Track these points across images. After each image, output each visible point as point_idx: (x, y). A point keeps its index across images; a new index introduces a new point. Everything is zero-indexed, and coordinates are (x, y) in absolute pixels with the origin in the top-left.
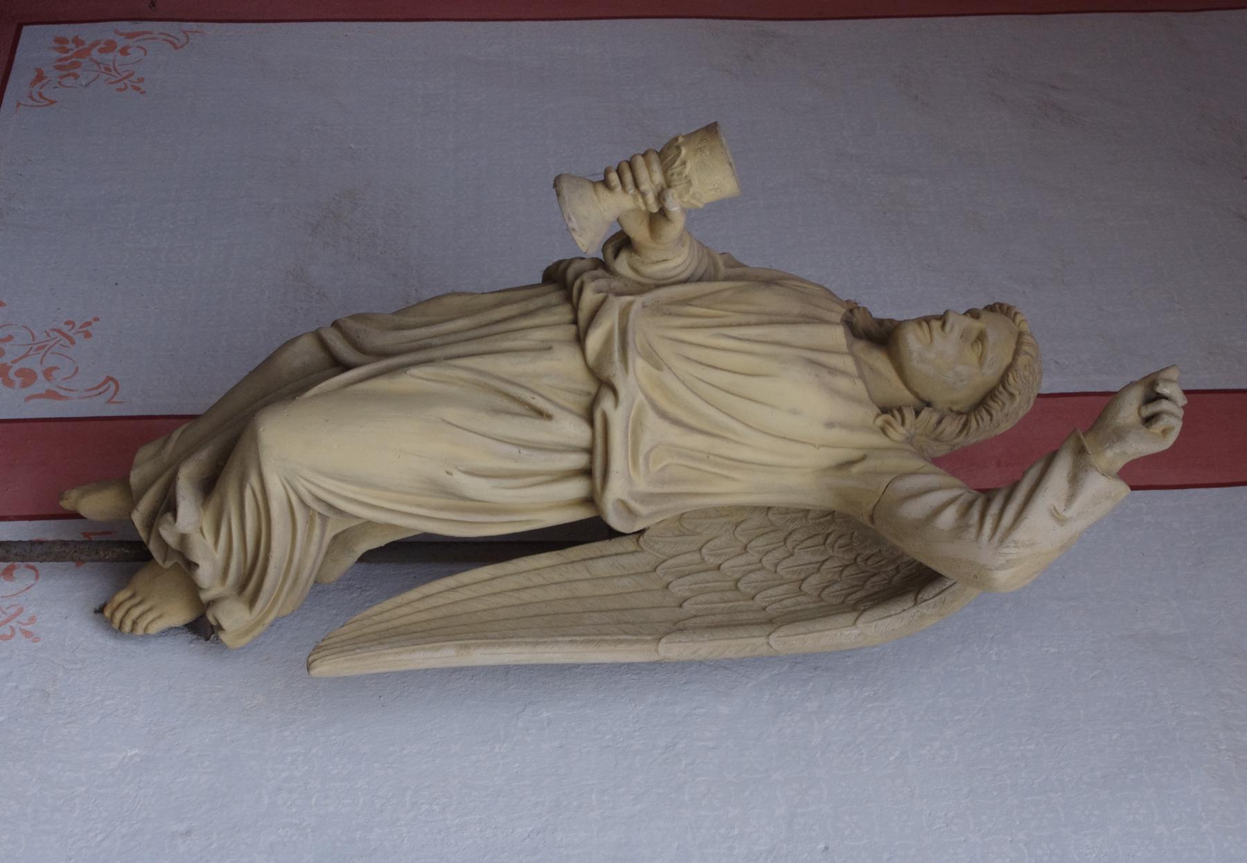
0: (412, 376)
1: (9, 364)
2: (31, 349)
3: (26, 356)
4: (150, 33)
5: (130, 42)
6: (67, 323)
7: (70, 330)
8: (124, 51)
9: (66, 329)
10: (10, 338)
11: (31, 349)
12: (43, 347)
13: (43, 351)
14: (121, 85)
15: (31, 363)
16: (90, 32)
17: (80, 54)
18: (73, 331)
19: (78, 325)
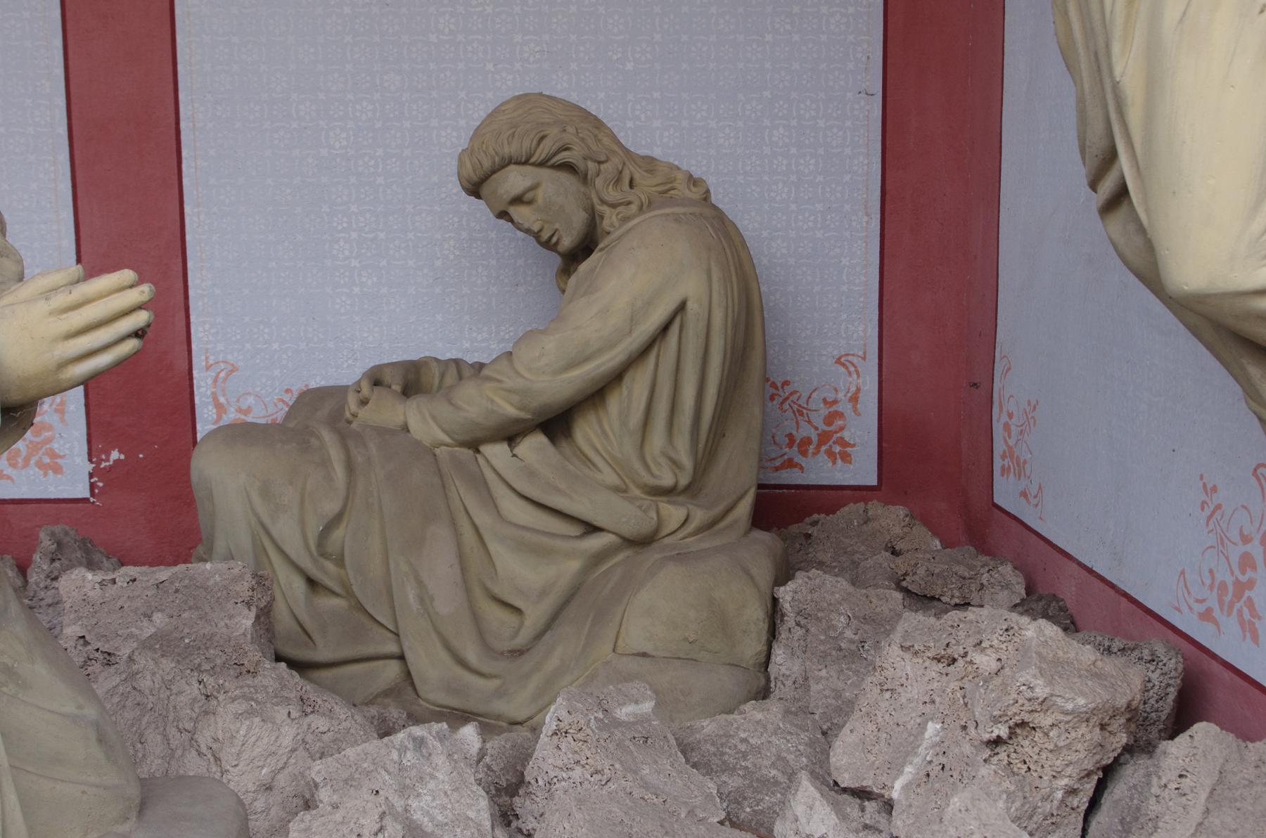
0: (1123, 74)
1: (1233, 579)
2: (1222, 552)
3: (1227, 558)
4: (1000, 389)
5: (1005, 409)
6: (1203, 509)
7: (1209, 507)
8: (1010, 416)
9: (1208, 512)
10: (1211, 571)
11: (1222, 552)
12: (1222, 539)
13: (1226, 541)
14: (1032, 422)
15: (1235, 554)
16: (999, 447)
17: (1012, 456)
18: (1210, 504)
19: (1204, 497)
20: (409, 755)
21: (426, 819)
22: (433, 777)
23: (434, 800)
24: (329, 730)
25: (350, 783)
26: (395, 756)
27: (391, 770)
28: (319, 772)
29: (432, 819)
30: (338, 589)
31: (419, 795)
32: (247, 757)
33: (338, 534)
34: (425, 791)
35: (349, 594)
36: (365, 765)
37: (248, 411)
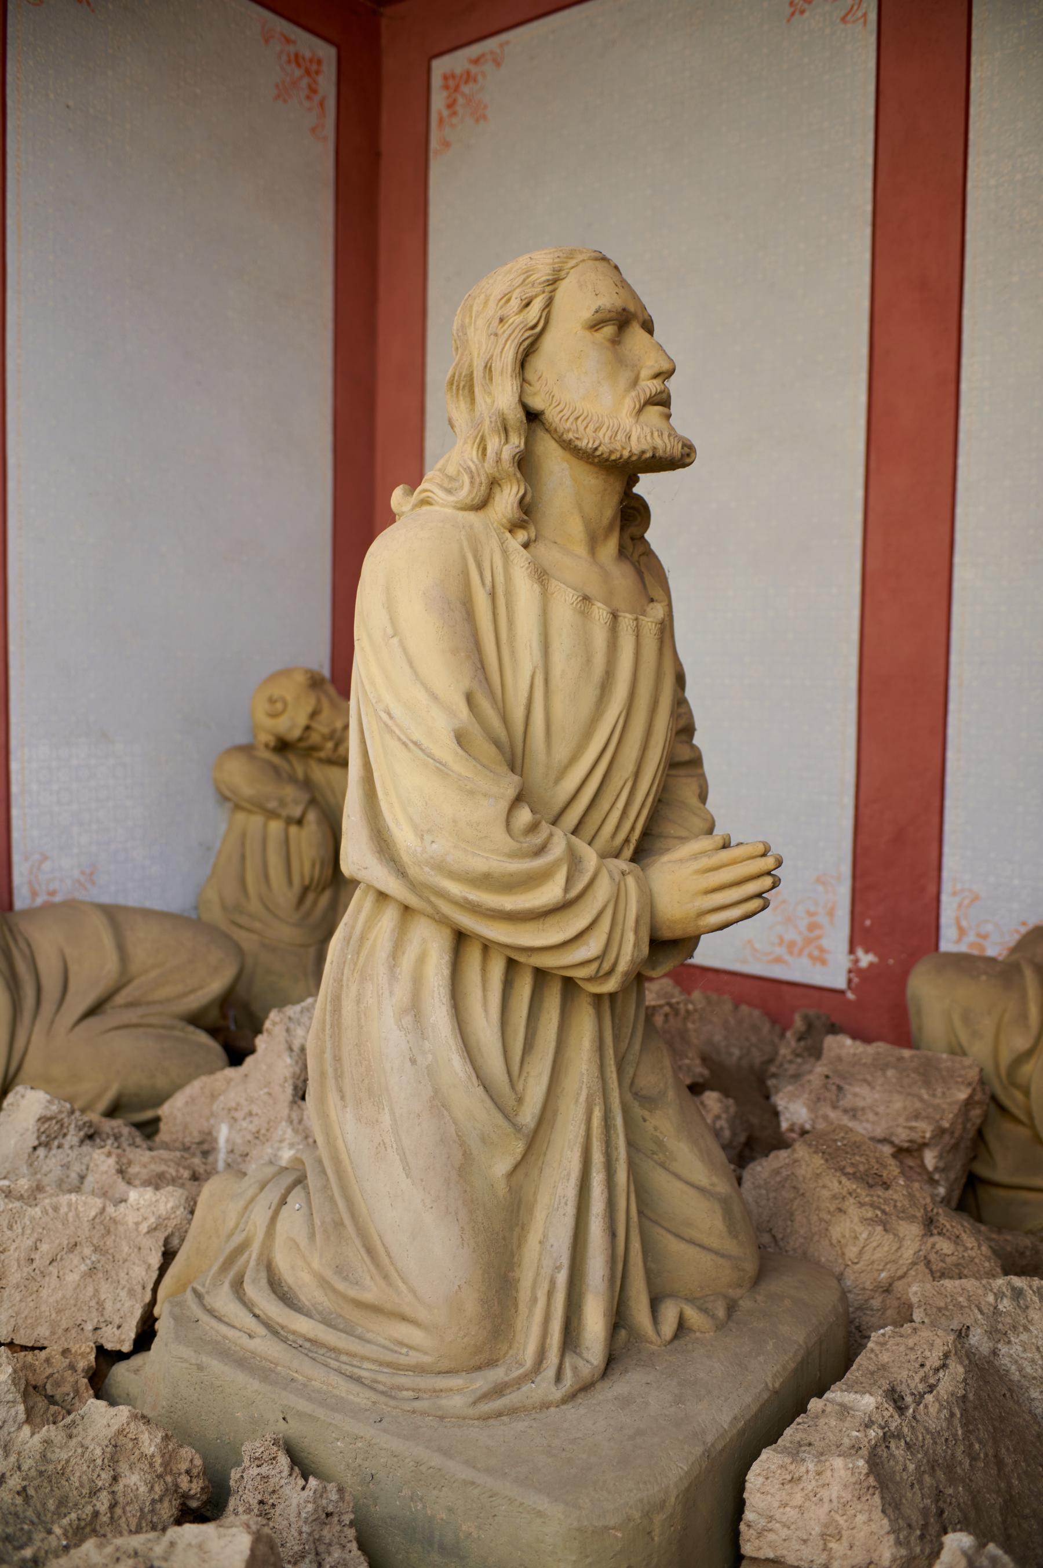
20: (1006, 1302)
21: (1014, 1367)
22: (1026, 1329)
23: (1025, 1351)
24: (953, 1254)
25: (943, 1312)
26: (991, 1298)
27: (986, 1311)
28: (916, 1293)
29: (1021, 1370)
30: (1023, 1117)
31: (1009, 1342)
32: (867, 1258)
33: (1027, 1068)
34: (1017, 1341)
35: (1033, 1127)
36: (961, 1299)
37: (985, 937)
